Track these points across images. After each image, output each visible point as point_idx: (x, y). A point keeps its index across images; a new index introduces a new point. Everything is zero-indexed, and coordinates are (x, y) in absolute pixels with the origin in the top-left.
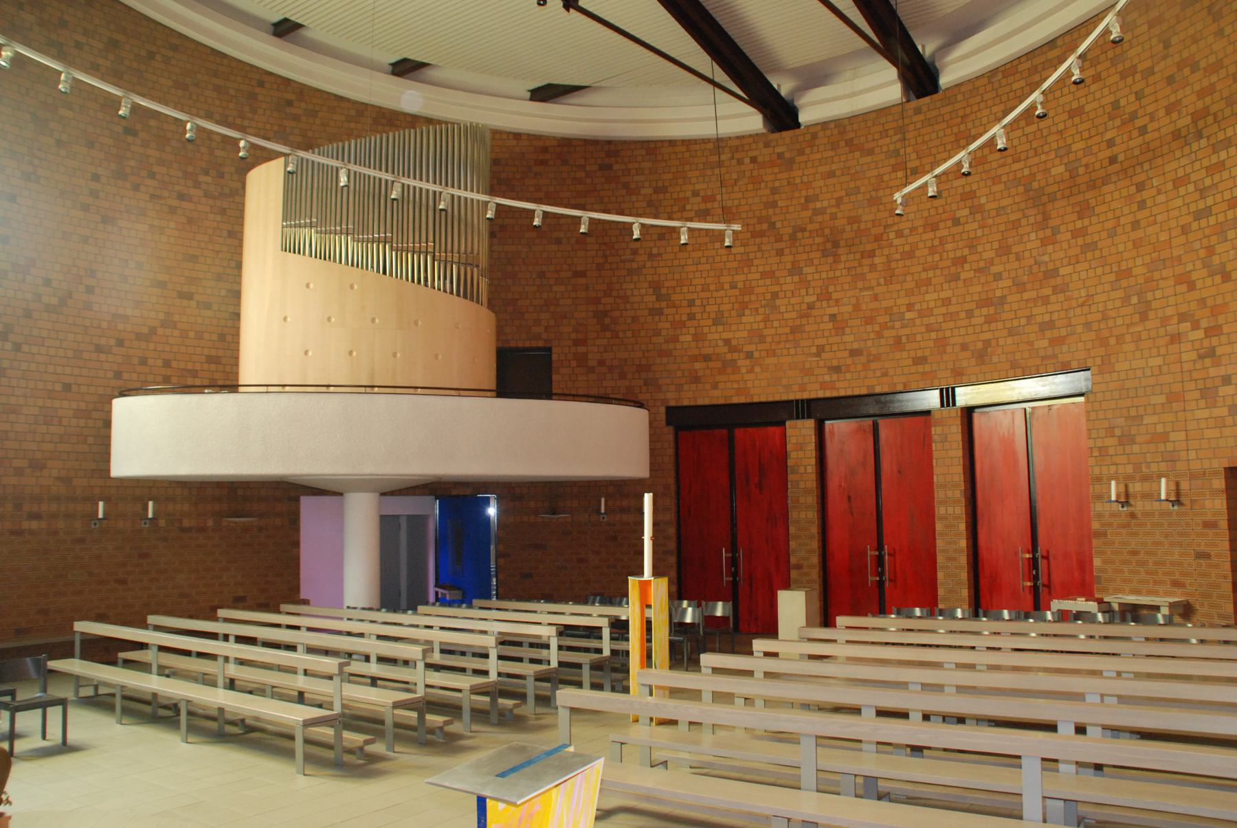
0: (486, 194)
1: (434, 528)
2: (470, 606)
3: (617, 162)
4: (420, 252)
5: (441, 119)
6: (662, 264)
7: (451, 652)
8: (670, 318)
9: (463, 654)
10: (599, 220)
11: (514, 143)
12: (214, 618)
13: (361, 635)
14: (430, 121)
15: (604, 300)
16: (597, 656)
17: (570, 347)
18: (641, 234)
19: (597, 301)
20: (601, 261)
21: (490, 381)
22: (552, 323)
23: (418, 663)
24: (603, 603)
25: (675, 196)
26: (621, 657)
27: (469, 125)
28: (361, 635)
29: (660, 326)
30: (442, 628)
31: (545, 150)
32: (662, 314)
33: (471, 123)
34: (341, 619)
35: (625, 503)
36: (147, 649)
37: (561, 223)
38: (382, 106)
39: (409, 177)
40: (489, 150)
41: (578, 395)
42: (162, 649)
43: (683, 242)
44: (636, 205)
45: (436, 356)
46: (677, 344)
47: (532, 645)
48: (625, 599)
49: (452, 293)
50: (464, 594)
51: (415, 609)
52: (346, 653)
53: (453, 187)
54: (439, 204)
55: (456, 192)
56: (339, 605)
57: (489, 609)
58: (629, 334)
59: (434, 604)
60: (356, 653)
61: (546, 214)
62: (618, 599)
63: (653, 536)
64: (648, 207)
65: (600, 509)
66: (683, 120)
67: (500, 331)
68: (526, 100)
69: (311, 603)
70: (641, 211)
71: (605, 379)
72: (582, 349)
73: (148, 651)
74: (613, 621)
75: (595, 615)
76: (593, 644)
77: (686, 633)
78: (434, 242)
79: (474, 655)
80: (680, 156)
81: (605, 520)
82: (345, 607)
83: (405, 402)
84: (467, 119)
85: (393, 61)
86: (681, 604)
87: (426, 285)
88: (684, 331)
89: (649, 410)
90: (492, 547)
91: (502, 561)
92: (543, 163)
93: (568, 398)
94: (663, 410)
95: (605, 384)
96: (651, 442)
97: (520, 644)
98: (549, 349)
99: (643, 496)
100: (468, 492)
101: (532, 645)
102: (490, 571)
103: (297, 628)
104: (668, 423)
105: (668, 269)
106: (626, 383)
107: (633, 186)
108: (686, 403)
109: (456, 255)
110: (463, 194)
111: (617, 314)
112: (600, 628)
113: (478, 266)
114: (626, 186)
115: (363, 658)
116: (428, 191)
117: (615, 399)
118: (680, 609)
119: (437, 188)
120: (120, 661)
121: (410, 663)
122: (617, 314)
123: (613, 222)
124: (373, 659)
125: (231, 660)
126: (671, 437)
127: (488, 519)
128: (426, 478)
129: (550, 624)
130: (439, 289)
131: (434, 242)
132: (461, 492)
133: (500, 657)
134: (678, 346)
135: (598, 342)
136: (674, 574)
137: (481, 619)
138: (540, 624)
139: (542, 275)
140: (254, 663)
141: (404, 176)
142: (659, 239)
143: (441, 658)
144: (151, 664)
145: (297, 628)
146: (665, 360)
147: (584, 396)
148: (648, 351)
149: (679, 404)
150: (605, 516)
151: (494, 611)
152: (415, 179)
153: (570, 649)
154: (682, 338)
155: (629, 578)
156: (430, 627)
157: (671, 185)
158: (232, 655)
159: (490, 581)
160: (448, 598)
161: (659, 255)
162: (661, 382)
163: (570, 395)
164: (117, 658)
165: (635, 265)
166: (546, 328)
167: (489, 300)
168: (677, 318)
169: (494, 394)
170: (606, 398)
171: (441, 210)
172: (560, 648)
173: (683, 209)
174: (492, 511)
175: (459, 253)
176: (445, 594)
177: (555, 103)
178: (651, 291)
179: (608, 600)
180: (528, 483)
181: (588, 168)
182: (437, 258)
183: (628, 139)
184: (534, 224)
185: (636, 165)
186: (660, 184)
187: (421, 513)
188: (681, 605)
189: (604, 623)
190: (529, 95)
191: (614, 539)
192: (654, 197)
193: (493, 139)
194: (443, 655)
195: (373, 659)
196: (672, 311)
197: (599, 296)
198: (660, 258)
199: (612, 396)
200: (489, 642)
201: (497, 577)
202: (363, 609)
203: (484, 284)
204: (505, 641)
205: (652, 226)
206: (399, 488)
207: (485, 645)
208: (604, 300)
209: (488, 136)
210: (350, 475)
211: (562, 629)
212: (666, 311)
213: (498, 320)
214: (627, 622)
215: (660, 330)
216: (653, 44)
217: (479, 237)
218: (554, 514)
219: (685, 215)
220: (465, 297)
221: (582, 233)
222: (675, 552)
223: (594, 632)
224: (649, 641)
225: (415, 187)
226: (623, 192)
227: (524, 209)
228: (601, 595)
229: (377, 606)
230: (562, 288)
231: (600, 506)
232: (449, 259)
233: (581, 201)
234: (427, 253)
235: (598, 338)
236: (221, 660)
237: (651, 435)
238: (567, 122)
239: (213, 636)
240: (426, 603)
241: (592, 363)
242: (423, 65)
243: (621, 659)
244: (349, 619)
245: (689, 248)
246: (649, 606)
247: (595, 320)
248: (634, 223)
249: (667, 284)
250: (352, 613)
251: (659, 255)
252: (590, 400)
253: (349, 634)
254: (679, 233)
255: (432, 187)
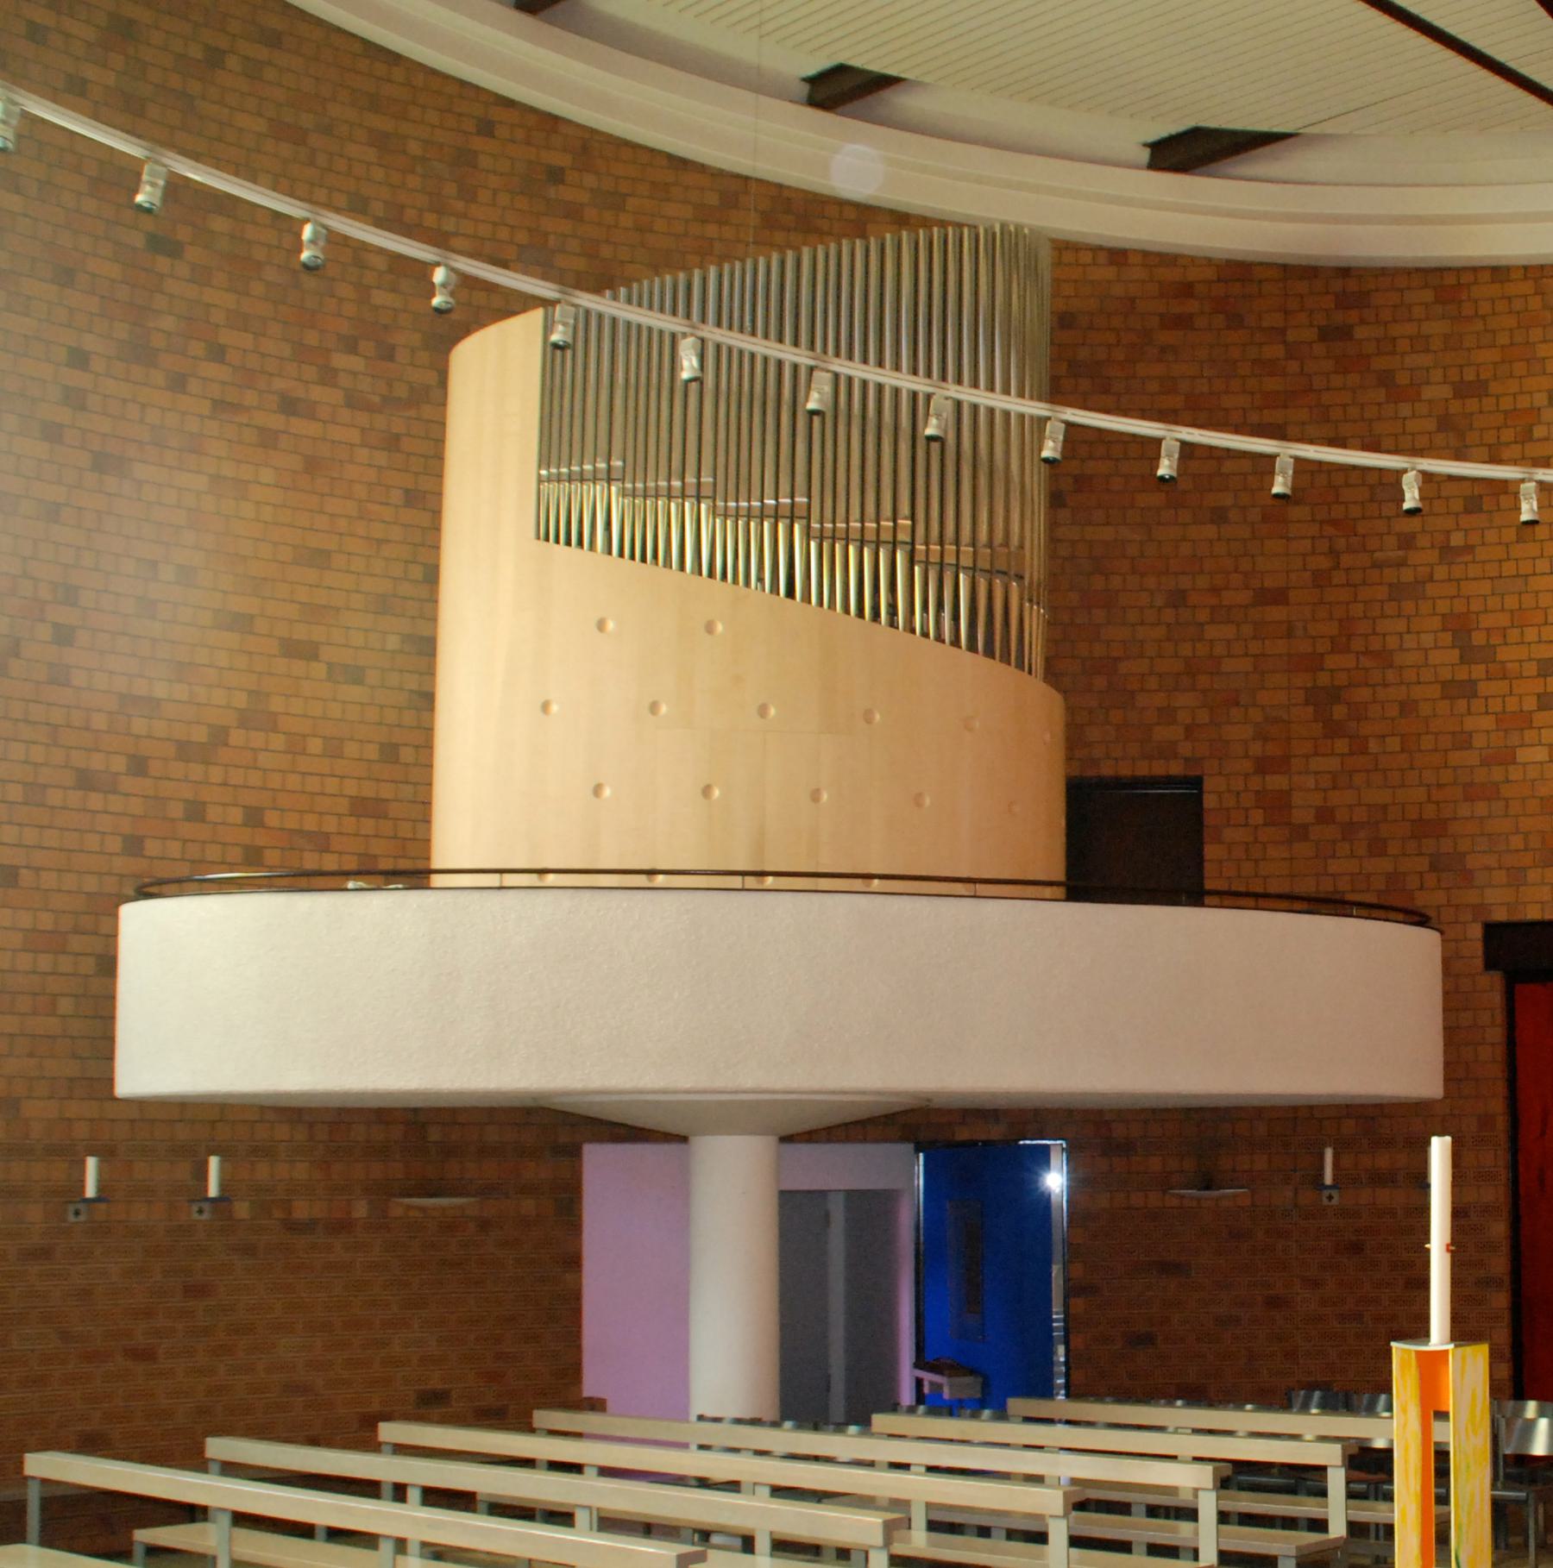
0: (1040, 399)
1: (912, 1223)
2: (1002, 1415)
3: (1363, 321)
4: (878, 544)
5: (928, 214)
6: (1473, 571)
7: (954, 1528)
8: (1496, 705)
9: (984, 1532)
10: (1320, 463)
11: (1110, 273)
12: (371, 1445)
13: (733, 1486)
14: (901, 219)
15: (1331, 661)
16: (1313, 1538)
17: (1247, 775)
18: (1422, 499)
19: (1314, 663)
20: (1324, 563)
21: (1051, 861)
22: (1203, 716)
23: (873, 1555)
24: (1328, 1406)
25: (1506, 403)
26: (1372, 1541)
27: (998, 230)
28: (733, 1486)
29: (1470, 724)
30: (932, 1469)
31: (1186, 290)
32: (1475, 695)
33: (1003, 226)
34: (684, 1446)
35: (1383, 1161)
36: (205, 1519)
37: (1224, 470)
38: (787, 182)
39: (850, 357)
40: (1047, 291)
41: (1266, 896)
42: (242, 1519)
43: (1525, 516)
44: (1412, 426)
45: (918, 800)
46: (1511, 768)
47: (1153, 1511)
48: (1383, 1397)
49: (956, 642)
50: (985, 1386)
51: (864, 1422)
52: (695, 1531)
53: (959, 381)
54: (926, 424)
55: (967, 395)
56: (679, 1410)
57: (1049, 1421)
58: (1394, 744)
59: (911, 1410)
60: (722, 1531)
61: (1188, 449)
62: (1366, 1398)
63: (1453, 1243)
64: (1439, 430)
65: (1321, 1175)
66: (1526, 218)
67: (1074, 738)
68: (1137, 167)
69: (609, 1405)
70: (1422, 441)
71: (1333, 857)
72: (1276, 782)
73: (208, 1526)
74: (1355, 1451)
75: (1308, 1437)
76: (1304, 1507)
77: (1533, 1481)
78: (913, 517)
79: (1012, 1535)
80: (1518, 305)
81: (1335, 1201)
82: (693, 1418)
83: (842, 908)
84: (993, 215)
85: (812, 71)
86: (1522, 1409)
87: (892, 623)
88: (1529, 735)
89: (1442, 933)
90: (1056, 1270)
91: (1079, 1304)
92: (1182, 322)
93: (1243, 901)
94: (1476, 931)
95: (1334, 866)
96: (1447, 1010)
97: (1123, 1508)
98: (1197, 782)
99: (1428, 1143)
100: (996, 1132)
101: (1153, 1511)
102: (1051, 1329)
103: (575, 1468)
104: (1490, 964)
105: (1488, 584)
106: (1384, 865)
107: (1403, 379)
108: (1533, 914)
109: (967, 550)
110: (983, 398)
111: (1363, 694)
112: (1323, 1469)
113: (1020, 577)
114: (1385, 379)
115: (738, 1542)
116: (896, 391)
117: (1360, 905)
118: (1519, 1423)
119: (921, 385)
120: (139, 1552)
121: (854, 1555)
122: (1363, 694)
123: (1354, 468)
124: (763, 1544)
125: (413, 1547)
126: (1497, 998)
127: (1045, 1200)
128: (894, 1099)
129: (1197, 1459)
130: (925, 634)
131: (913, 517)
132: (980, 1133)
133: (1076, 1541)
134: (1515, 773)
135: (1317, 763)
136: (1503, 1334)
137: (1027, 1447)
138: (1173, 1458)
139: (1178, 599)
140: (468, 1555)
141: (837, 355)
142: (1468, 511)
143: (931, 1543)
144: (214, 1558)
145: (575, 1468)
146: (1481, 808)
147: (1280, 897)
148: (1440, 786)
149: (1518, 917)
150: (1335, 1193)
151: (1060, 1427)
152: (865, 361)
153: (1248, 1519)
154: (1523, 755)
155: (1393, 1344)
156: (904, 1467)
157: (1495, 378)
158: (415, 1535)
159: (1049, 1354)
160: (946, 1393)
161: (1469, 549)
162: (1472, 862)
163: (1247, 895)
164: (131, 1543)
165: (1407, 575)
166: (1189, 730)
167: (1049, 662)
168: (1512, 705)
169: (1060, 892)
170: (1335, 902)
171: (930, 439)
172: (1223, 1517)
173: (1526, 437)
174: (1055, 1181)
175: (974, 545)
176: (940, 1386)
177: (1209, 175)
178: (1447, 638)
179: (1341, 1400)
180: (1143, 1110)
181: (1291, 336)
182: (920, 557)
183: (1390, 264)
184: (1160, 472)
185: (1410, 329)
186: (1470, 376)
187: (880, 1185)
188: (1519, 1412)
189: (1330, 1456)
190: (1145, 155)
191: (1356, 1248)
192: (1455, 407)
193: (1058, 264)
194: (934, 1535)
195: (763, 1544)
196: (1499, 687)
197: (1320, 650)
198: (1469, 558)
199: (1350, 897)
200: (1048, 1503)
201: (1067, 1343)
202: (738, 1421)
203: (1035, 620)
204: (1085, 1501)
205: (1451, 478)
206: (826, 1122)
207: (1038, 1511)
208: (1331, 661)
209: (1046, 257)
210: (705, 1092)
211: (1227, 1470)
212: (1484, 688)
213: (1071, 710)
214: (1388, 1453)
215: (1470, 734)
216: (1452, 30)
217: (1023, 505)
218: (1208, 1188)
219: (1533, 450)
220: (989, 652)
221: (1277, 496)
222: (1507, 1279)
223: (1306, 1479)
224: (1443, 1500)
225: (865, 383)
226: (1380, 396)
227: (1134, 436)
228: (1325, 1387)
229: (771, 1413)
230: (1228, 631)
231: (1321, 1168)
232: (950, 559)
233: (1276, 416)
234: (894, 544)
235: (1316, 754)
236: (386, 1548)
237: (1446, 994)
238: (1266, 224)
239: (367, 1488)
240: (894, 1408)
241: (1301, 816)
242: (884, 82)
243: (1373, 1544)
244: (702, 1447)
245: (1541, 532)
246: (1442, 1415)
247: (1311, 709)
248: (1405, 471)
249: (1487, 621)
250: (709, 1433)
251: (1469, 549)
252: (1297, 905)
253: (704, 1483)
254: (1516, 496)
255: (907, 382)
